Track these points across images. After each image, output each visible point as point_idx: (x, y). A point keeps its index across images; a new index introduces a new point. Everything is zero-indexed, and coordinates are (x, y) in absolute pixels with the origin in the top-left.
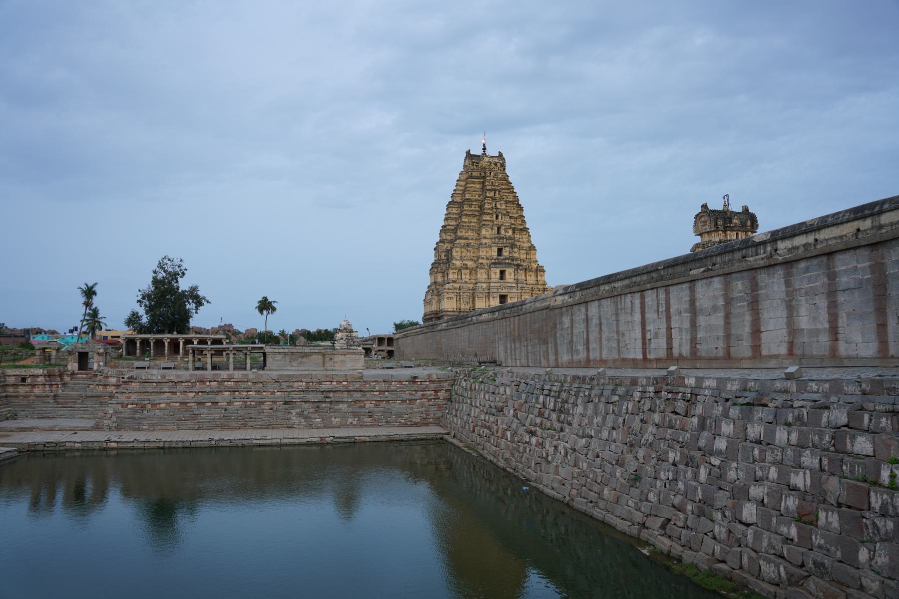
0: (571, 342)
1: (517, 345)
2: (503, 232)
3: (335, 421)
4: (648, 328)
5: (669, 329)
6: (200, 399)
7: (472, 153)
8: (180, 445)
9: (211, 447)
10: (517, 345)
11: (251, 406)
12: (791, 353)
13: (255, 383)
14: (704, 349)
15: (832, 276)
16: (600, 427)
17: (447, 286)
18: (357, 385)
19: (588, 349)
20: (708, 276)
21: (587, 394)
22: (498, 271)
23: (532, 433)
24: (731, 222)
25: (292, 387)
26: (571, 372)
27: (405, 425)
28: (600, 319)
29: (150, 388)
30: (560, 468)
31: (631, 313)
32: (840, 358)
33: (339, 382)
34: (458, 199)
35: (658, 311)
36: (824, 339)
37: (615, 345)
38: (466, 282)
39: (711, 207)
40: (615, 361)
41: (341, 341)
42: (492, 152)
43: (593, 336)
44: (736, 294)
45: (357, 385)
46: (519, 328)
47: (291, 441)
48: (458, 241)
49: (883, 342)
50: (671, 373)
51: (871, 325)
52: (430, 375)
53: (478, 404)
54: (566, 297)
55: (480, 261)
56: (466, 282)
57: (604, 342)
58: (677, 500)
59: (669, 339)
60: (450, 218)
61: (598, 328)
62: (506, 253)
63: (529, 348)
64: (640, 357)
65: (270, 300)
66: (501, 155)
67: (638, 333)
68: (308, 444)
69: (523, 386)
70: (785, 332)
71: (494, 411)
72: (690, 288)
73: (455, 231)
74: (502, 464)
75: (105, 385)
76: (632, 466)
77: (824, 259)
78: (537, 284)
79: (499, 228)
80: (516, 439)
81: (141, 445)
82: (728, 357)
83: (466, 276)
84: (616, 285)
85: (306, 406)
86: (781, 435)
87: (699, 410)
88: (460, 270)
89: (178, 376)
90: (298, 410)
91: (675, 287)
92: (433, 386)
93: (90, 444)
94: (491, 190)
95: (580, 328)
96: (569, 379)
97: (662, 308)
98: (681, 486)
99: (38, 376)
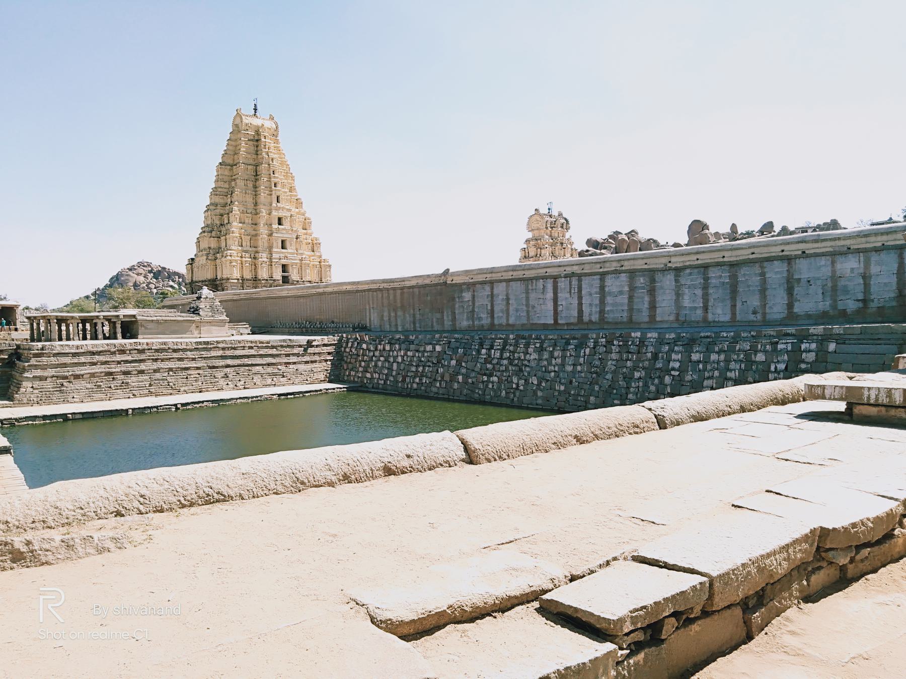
0: (473, 311)
1: (400, 313)
4: (559, 303)
5: (580, 304)
12: (677, 320)
15: (706, 279)
16: (563, 365)
19: (492, 317)
21: (538, 345)
23: (491, 375)
28: (507, 295)
31: (543, 293)
32: (710, 323)
34: (230, 161)
36: (699, 312)
37: (525, 314)
40: (523, 325)
44: (638, 284)
46: (402, 299)
49: (734, 314)
51: (729, 303)
53: (400, 359)
57: (511, 312)
59: (580, 312)
61: (505, 303)
67: (550, 305)
72: (601, 279)
76: (606, 384)
77: (702, 270)
80: (470, 381)
86: (714, 357)
87: (651, 349)
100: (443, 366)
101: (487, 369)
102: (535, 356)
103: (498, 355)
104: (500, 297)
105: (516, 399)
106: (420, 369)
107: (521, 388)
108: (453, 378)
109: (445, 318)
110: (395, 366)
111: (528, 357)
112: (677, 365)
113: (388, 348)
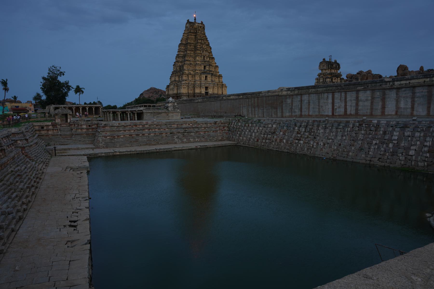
0: (292, 108)
1: (256, 109)
2: (206, 59)
3: (192, 140)
4: (335, 105)
5: (346, 106)
6: (136, 133)
7: (190, 21)
8: (145, 152)
9: (157, 152)
10: (256, 109)
11: (157, 135)
13: (157, 125)
14: (360, 112)
16: (336, 136)
17: (183, 82)
18: (196, 125)
19: (301, 111)
20: (365, 90)
21: (324, 126)
22: (204, 76)
23: (300, 140)
24: (333, 66)
25: (171, 127)
26: (311, 120)
27: (216, 141)
28: (309, 101)
29: (114, 129)
30: (324, 149)
31: (327, 100)
33: (189, 124)
34: (184, 43)
35: (341, 99)
37: (317, 110)
38: (191, 81)
39: (326, 60)
40: (316, 115)
42: (198, 21)
45: (196, 125)
47: (186, 148)
48: (186, 62)
50: (365, 119)
53: (256, 131)
54: (289, 92)
55: (197, 71)
56: (191, 81)
58: (382, 153)
60: (181, 51)
62: (207, 68)
63: (265, 110)
64: (331, 114)
65: (81, 87)
66: (202, 23)
67: (330, 106)
68: (192, 149)
69: (282, 124)
71: (270, 133)
73: (184, 56)
74: (286, 151)
75: (82, 129)
78: (219, 82)
79: (204, 57)
80: (289, 142)
81: (129, 153)
83: (190, 78)
84: (319, 89)
85: (179, 134)
87: (382, 129)
88: (188, 75)
89: (125, 123)
90: (177, 136)
91: (350, 92)
93: (108, 154)
94: (200, 39)
96: (310, 121)
97: (343, 98)
98: (382, 149)
99: (49, 126)
100: (276, 135)
101: (298, 137)
102: (322, 131)
103: (304, 130)
104: (305, 102)
105: (312, 152)
106: (266, 136)
107: (315, 147)
108: (281, 141)
109: (278, 111)
110: (253, 135)
111: (318, 131)
112: (396, 138)
113: (250, 125)
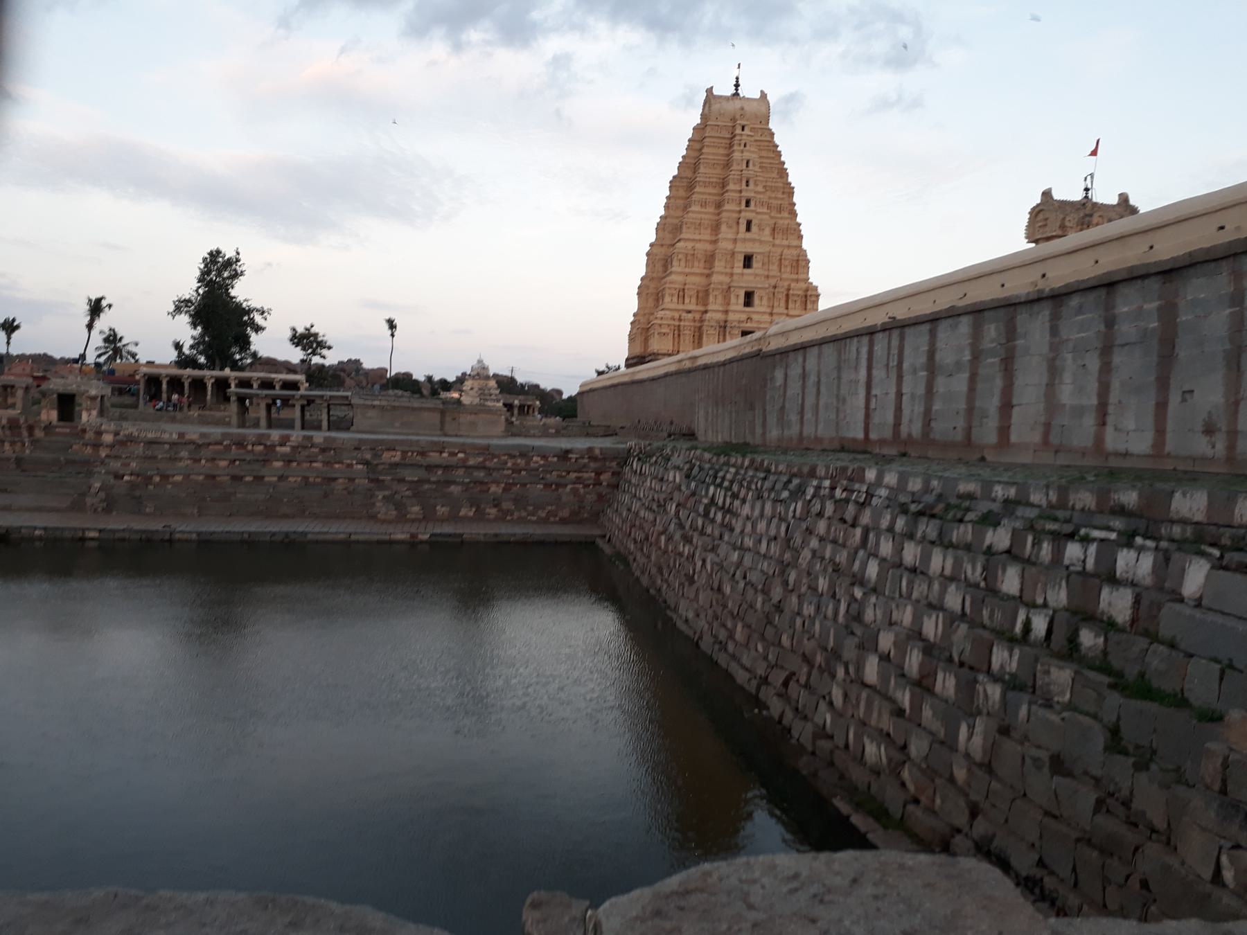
0: (783, 408)
2: (754, 228)
4: (874, 392)
5: (900, 395)
7: (715, 92)
12: (1046, 442)
13: (323, 450)
14: (940, 428)
15: (1110, 323)
23: (687, 540)
27: (544, 521)
28: (819, 376)
34: (689, 174)
35: (887, 365)
36: (1089, 421)
37: (833, 416)
39: (1058, 195)
41: (472, 393)
43: (810, 401)
52: (590, 449)
64: (861, 436)
66: (764, 95)
70: (1041, 406)
72: (931, 331)
77: (1103, 292)
82: (968, 442)
90: (387, 493)
92: (592, 465)
95: (794, 388)
